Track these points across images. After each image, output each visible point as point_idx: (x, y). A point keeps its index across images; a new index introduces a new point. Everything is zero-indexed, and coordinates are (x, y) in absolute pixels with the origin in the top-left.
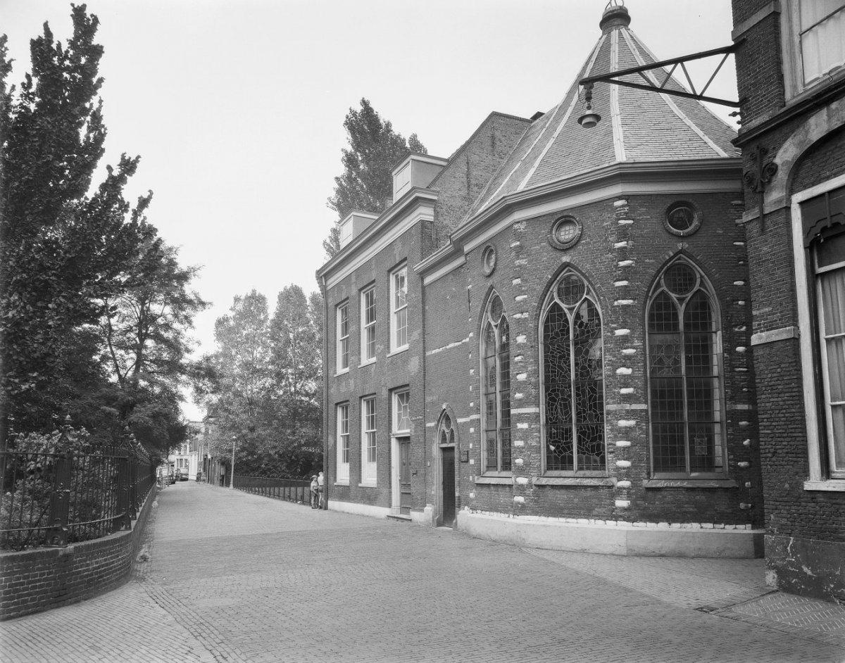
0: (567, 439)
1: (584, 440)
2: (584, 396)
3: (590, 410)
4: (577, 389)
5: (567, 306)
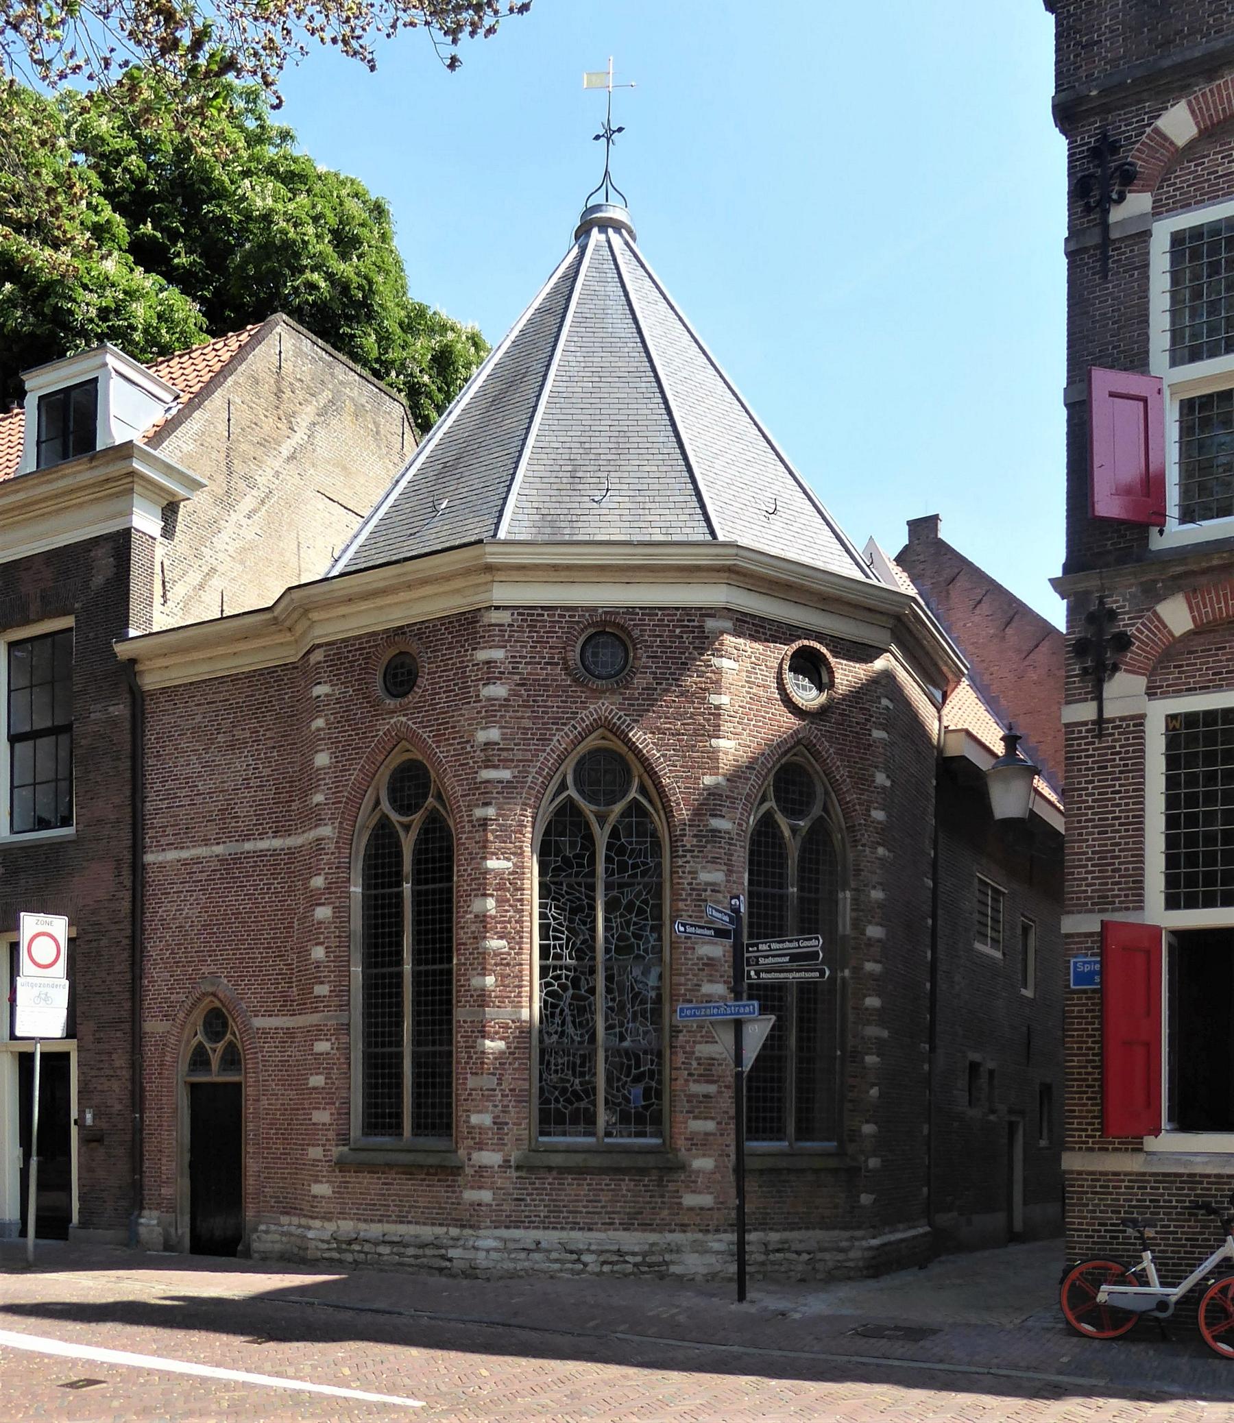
0: (582, 1074)
1: (619, 1079)
2: (621, 994)
3: (634, 1019)
4: (609, 979)
5: (593, 808)
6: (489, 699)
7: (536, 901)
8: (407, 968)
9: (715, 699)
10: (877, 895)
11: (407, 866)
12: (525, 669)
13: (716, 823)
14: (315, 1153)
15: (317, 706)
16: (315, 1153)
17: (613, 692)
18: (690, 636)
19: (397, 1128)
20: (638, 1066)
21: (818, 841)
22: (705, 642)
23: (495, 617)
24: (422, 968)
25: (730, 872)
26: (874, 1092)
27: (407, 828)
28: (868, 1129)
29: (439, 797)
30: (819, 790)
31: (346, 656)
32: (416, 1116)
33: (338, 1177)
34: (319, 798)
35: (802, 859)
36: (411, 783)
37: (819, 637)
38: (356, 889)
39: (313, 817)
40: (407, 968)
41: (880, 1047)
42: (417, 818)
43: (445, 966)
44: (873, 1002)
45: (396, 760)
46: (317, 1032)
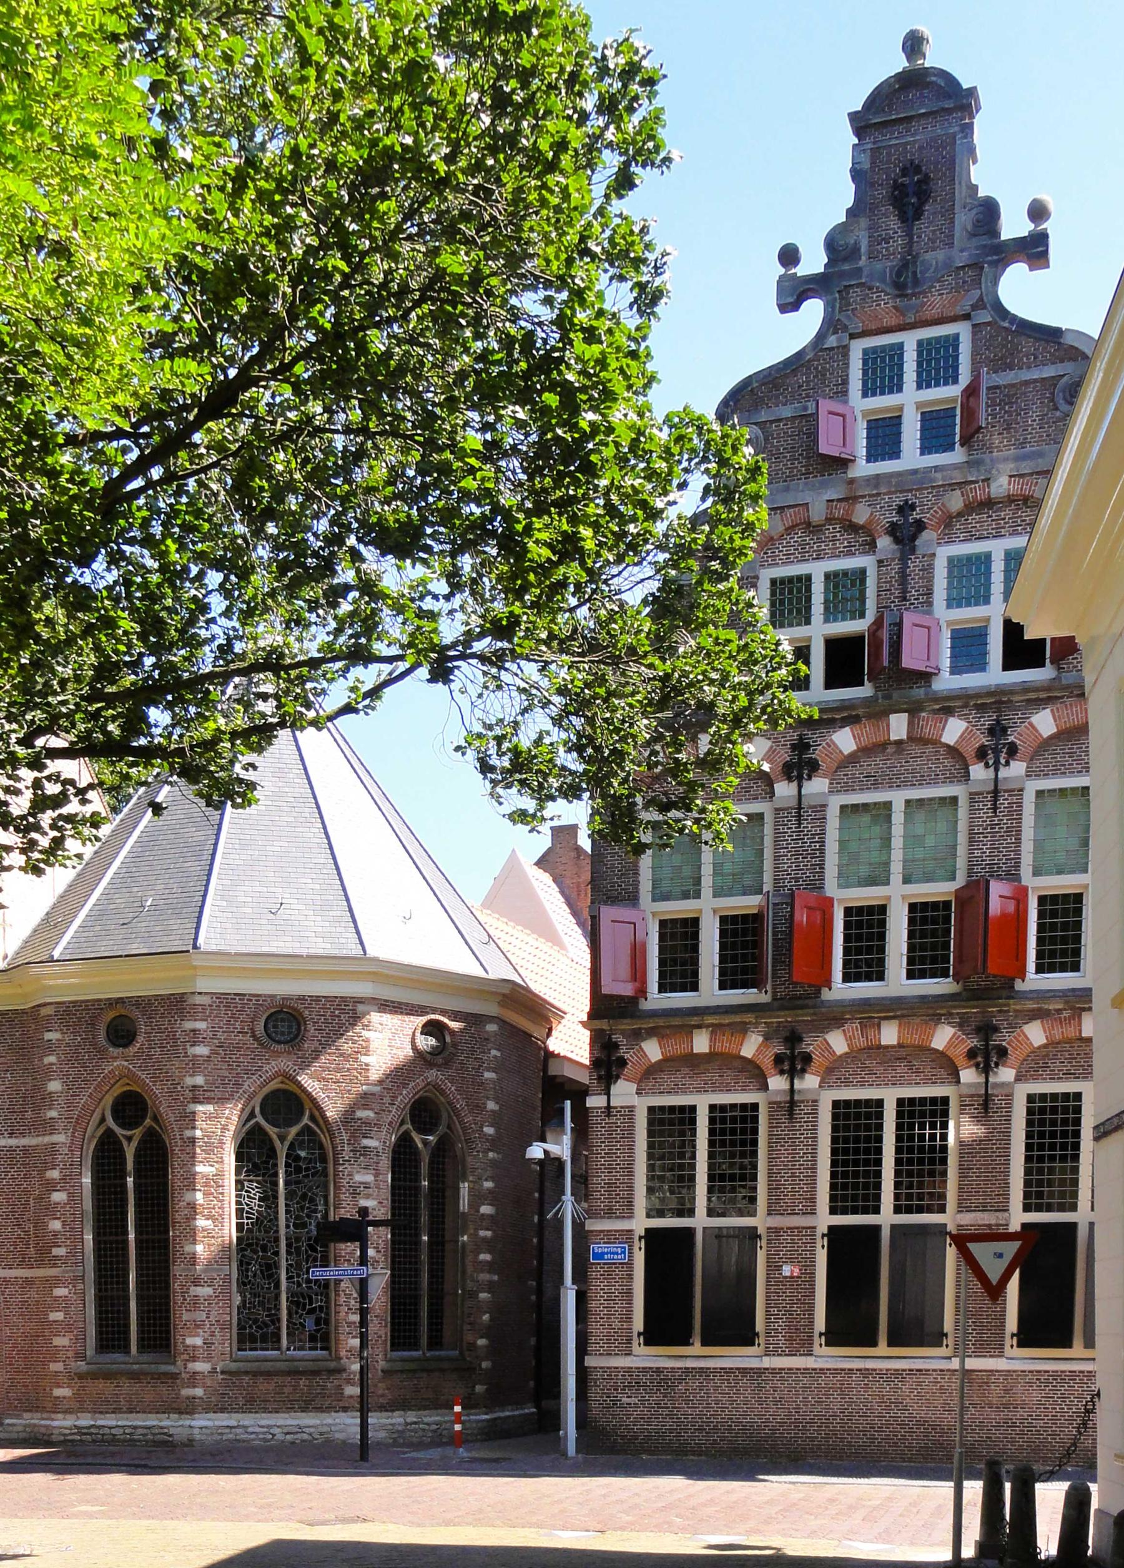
6: (195, 1056)
7: (233, 1193)
8: (132, 1236)
9: (364, 1059)
10: (489, 1185)
11: (130, 1165)
12: (222, 1036)
13: (366, 1142)
14: (55, 1367)
15: (49, 1048)
16: (55, 1367)
17: (289, 1053)
18: (345, 1014)
19: (126, 1349)
20: (311, 1303)
21: (442, 1151)
22: (355, 1018)
23: (198, 1000)
24: (145, 1237)
25: (376, 1175)
26: (486, 1317)
27: (129, 1139)
28: (482, 1342)
29: (155, 1119)
30: (444, 1115)
31: (76, 1014)
32: (141, 1340)
33: (77, 1383)
34: (53, 1114)
35: (431, 1163)
36: (131, 1107)
37: (443, 1012)
38: (87, 1180)
39: (50, 1127)
40: (132, 1236)
41: (490, 1287)
42: (137, 1133)
43: (163, 1237)
44: (485, 1257)
45: (118, 1090)
46: (56, 1282)
